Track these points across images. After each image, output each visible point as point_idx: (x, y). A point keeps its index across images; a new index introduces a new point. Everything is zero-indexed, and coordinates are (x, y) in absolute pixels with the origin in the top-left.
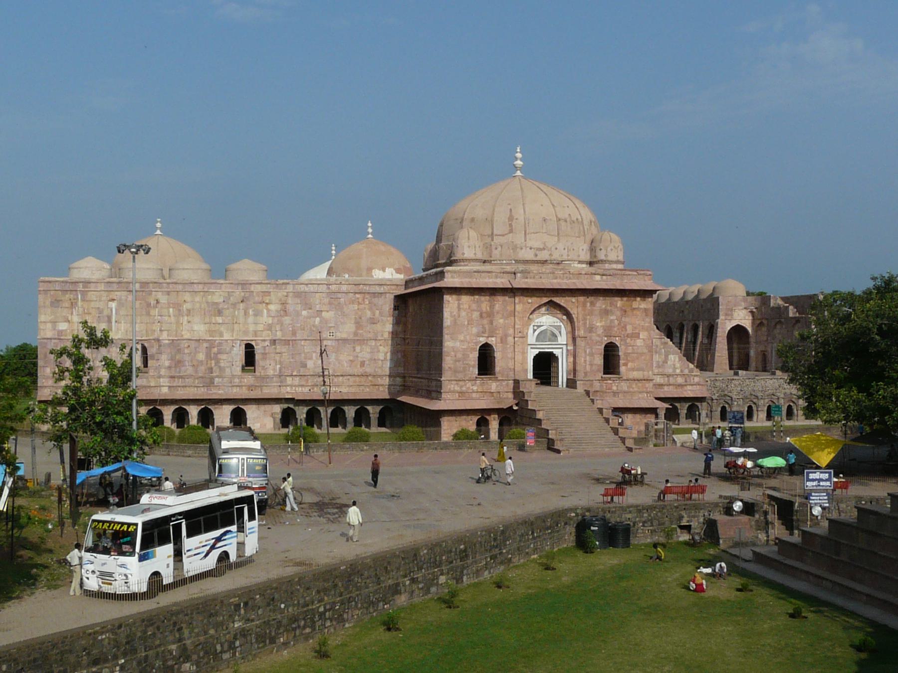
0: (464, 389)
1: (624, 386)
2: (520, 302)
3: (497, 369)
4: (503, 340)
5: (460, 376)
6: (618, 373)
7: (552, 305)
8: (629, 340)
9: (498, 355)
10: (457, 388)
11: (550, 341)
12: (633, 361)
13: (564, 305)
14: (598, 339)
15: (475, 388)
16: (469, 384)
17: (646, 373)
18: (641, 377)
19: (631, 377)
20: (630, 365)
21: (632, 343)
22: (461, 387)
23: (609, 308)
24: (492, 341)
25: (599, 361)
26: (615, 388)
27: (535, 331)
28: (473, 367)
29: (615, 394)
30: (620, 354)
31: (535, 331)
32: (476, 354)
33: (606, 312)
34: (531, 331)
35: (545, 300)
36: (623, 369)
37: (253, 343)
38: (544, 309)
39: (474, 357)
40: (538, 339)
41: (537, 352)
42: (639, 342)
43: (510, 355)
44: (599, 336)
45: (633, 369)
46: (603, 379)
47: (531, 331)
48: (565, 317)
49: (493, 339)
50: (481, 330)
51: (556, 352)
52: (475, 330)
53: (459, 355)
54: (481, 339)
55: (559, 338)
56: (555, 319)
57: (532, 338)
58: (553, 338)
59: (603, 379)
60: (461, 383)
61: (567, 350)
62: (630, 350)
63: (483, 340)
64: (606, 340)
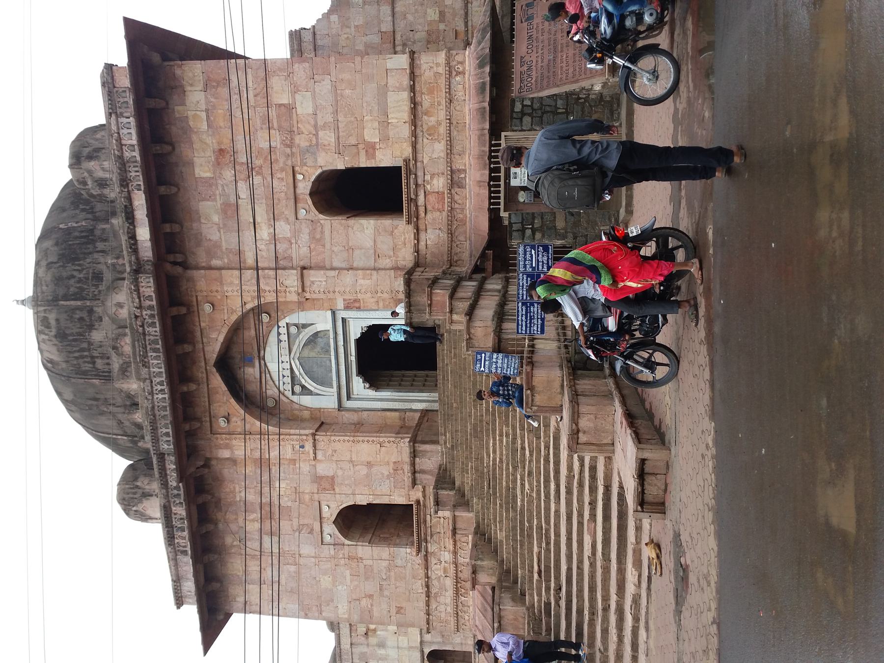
0: (449, 583)
1: (433, 151)
2: (227, 447)
3: (399, 499)
4: (327, 484)
5: (419, 586)
6: (394, 172)
7: (227, 365)
8: (301, 141)
9: (362, 501)
10: (448, 597)
11: (328, 351)
12: (360, 124)
13: (225, 330)
14: (305, 237)
15: (447, 556)
16: (436, 570)
17: (392, 81)
18: (405, 95)
19: (406, 131)
20: (371, 135)
21: (307, 128)
22: (443, 588)
23: (219, 202)
24: (331, 512)
25: (366, 232)
26: (439, 184)
27: (305, 391)
28: (392, 558)
29: (455, 181)
30: (341, 166)
31: (305, 391)
32: (365, 551)
33: (232, 210)
34: (307, 401)
35: (217, 381)
36: (384, 159)
37: (427, 651)
38: (251, 372)
39: (371, 554)
40: (324, 382)
41: (358, 384)
42: (304, 107)
43: (364, 471)
44: (296, 233)
45: (385, 124)
46: (415, 220)
47: (307, 401)
48: (265, 318)
49: (325, 509)
50: (304, 534)
51: (355, 332)
52: (307, 550)
53: (370, 587)
54: (327, 538)
55: (320, 327)
56: (273, 338)
57: (325, 400)
58: (320, 341)
59: (415, 220)
60: (434, 590)
61: (347, 308)
62: (328, 137)
63: (330, 529)
64: (308, 209)
